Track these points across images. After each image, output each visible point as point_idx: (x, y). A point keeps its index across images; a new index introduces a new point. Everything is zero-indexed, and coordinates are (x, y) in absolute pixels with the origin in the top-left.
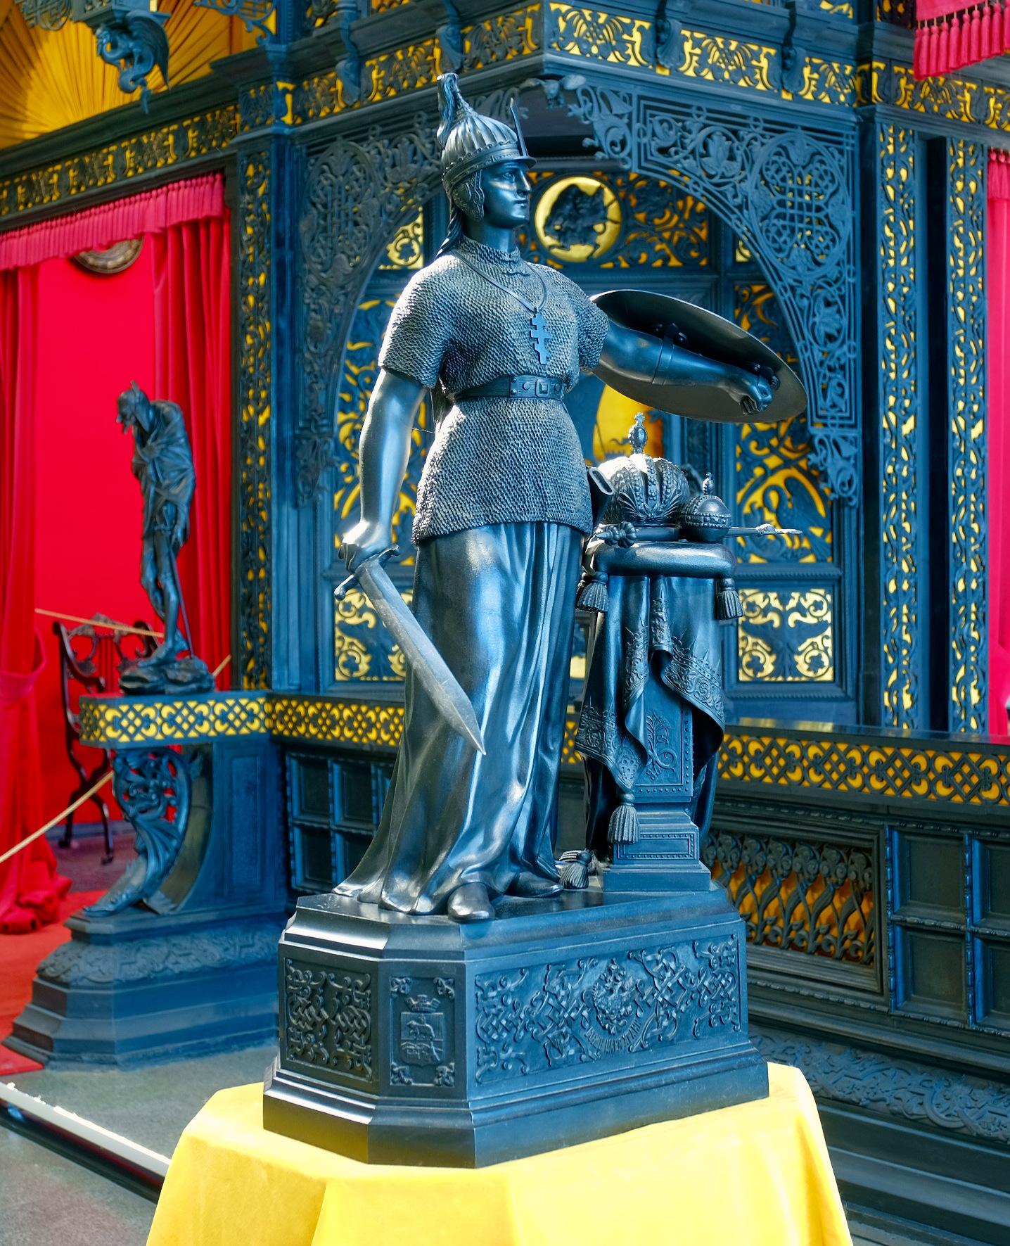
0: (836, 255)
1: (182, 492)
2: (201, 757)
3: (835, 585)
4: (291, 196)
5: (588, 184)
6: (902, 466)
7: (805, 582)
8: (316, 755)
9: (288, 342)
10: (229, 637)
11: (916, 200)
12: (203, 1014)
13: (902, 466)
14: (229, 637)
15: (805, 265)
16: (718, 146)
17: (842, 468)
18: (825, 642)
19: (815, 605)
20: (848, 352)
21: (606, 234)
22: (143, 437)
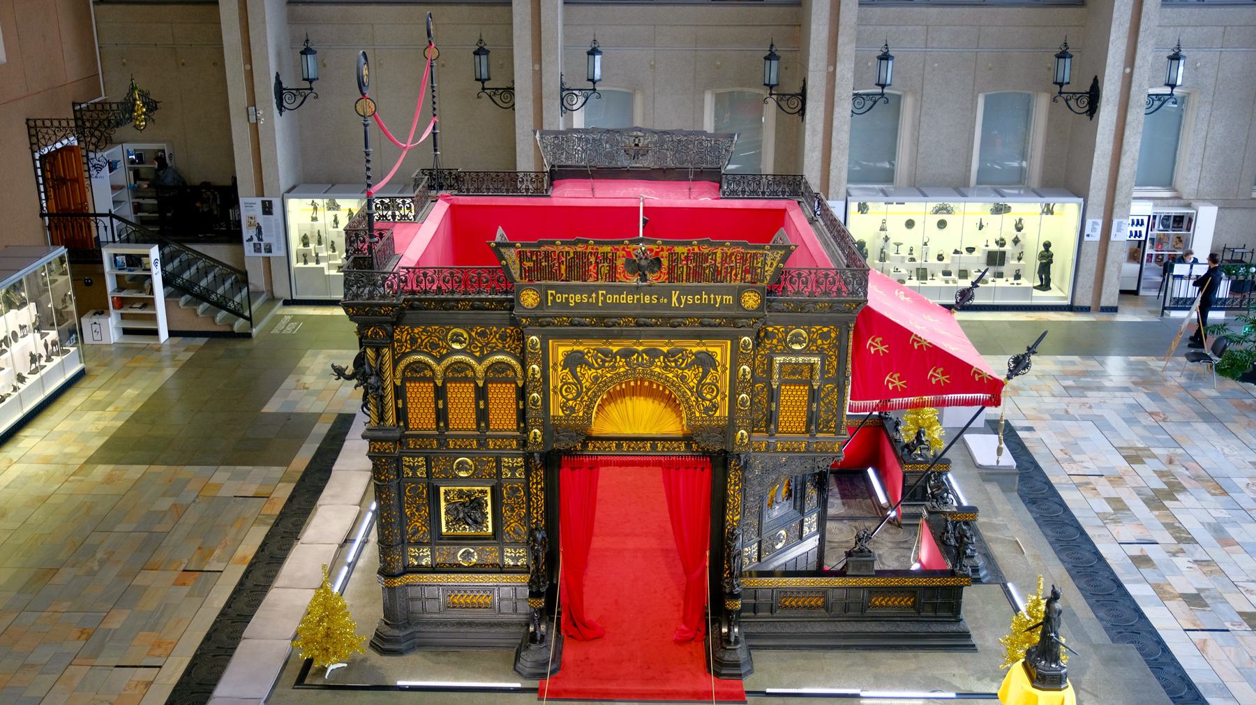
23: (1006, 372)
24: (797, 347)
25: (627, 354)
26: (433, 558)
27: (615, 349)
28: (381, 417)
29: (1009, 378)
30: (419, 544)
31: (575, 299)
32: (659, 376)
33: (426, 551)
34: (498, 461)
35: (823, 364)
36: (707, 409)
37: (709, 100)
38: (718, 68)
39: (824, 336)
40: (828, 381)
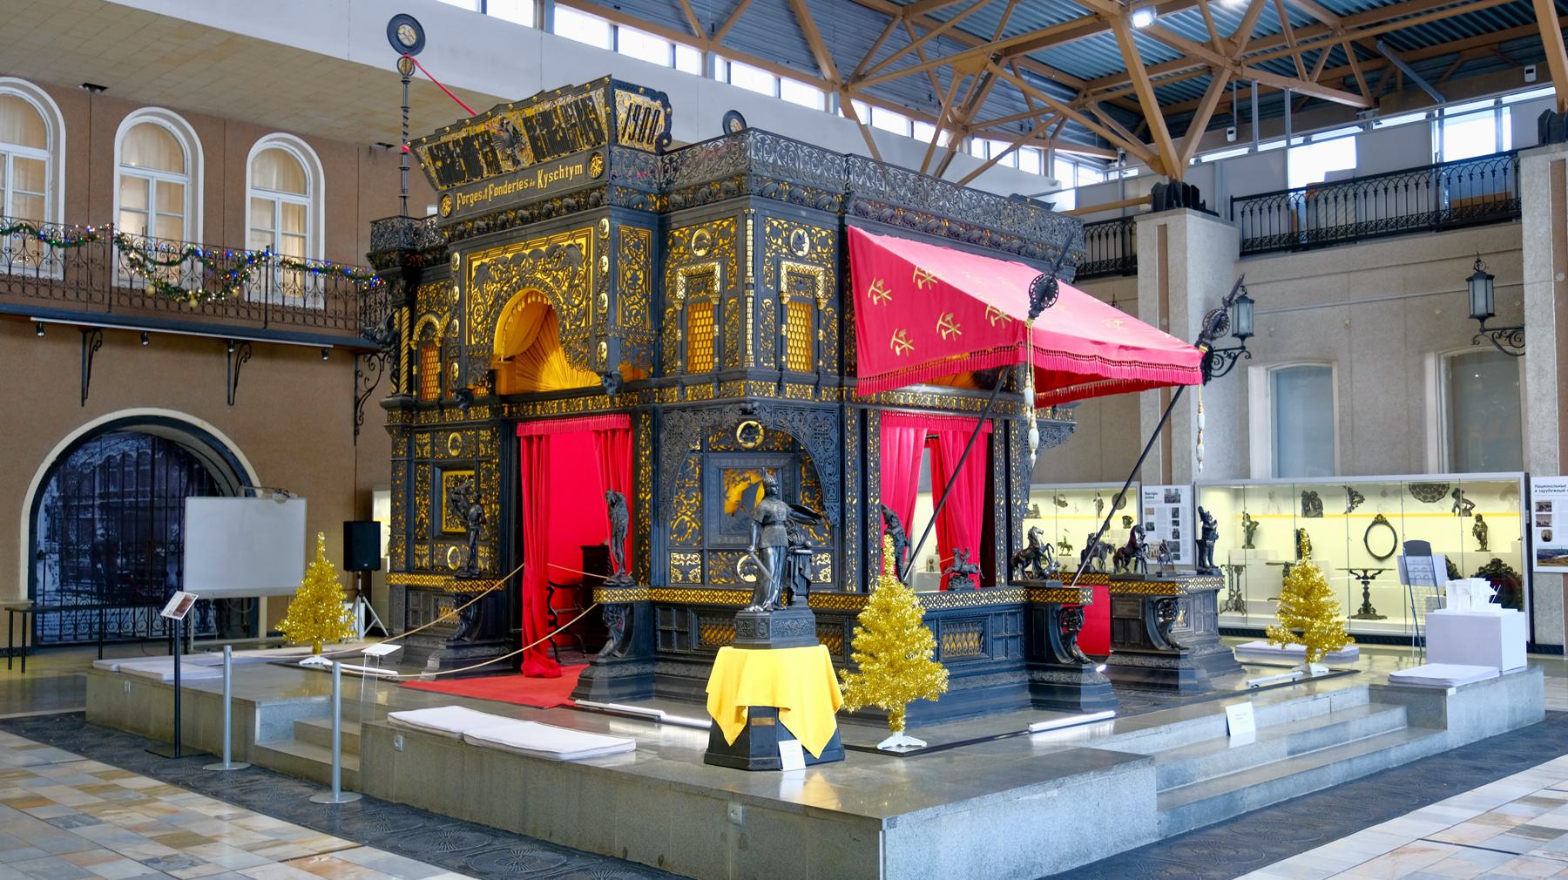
0: (833, 449)
1: (626, 521)
2: (629, 606)
3: (832, 552)
4: (657, 426)
5: (753, 423)
6: (853, 514)
7: (822, 551)
8: (667, 606)
9: (656, 473)
10: (641, 571)
11: (857, 430)
12: (634, 689)
13: (853, 514)
14: (641, 571)
15: (822, 453)
16: (797, 418)
17: (834, 516)
18: (829, 570)
19: (825, 558)
20: (836, 479)
21: (760, 439)
22: (613, 504)
23: (1028, 307)
24: (701, 253)
25: (518, 259)
26: (432, 557)
27: (509, 256)
28: (398, 386)
29: (1032, 316)
30: (422, 541)
31: (474, 197)
32: (542, 284)
33: (425, 549)
34: (477, 436)
35: (723, 272)
36: (576, 318)
37: (1430, 363)
38: (1438, 318)
39: (724, 233)
40: (732, 294)
